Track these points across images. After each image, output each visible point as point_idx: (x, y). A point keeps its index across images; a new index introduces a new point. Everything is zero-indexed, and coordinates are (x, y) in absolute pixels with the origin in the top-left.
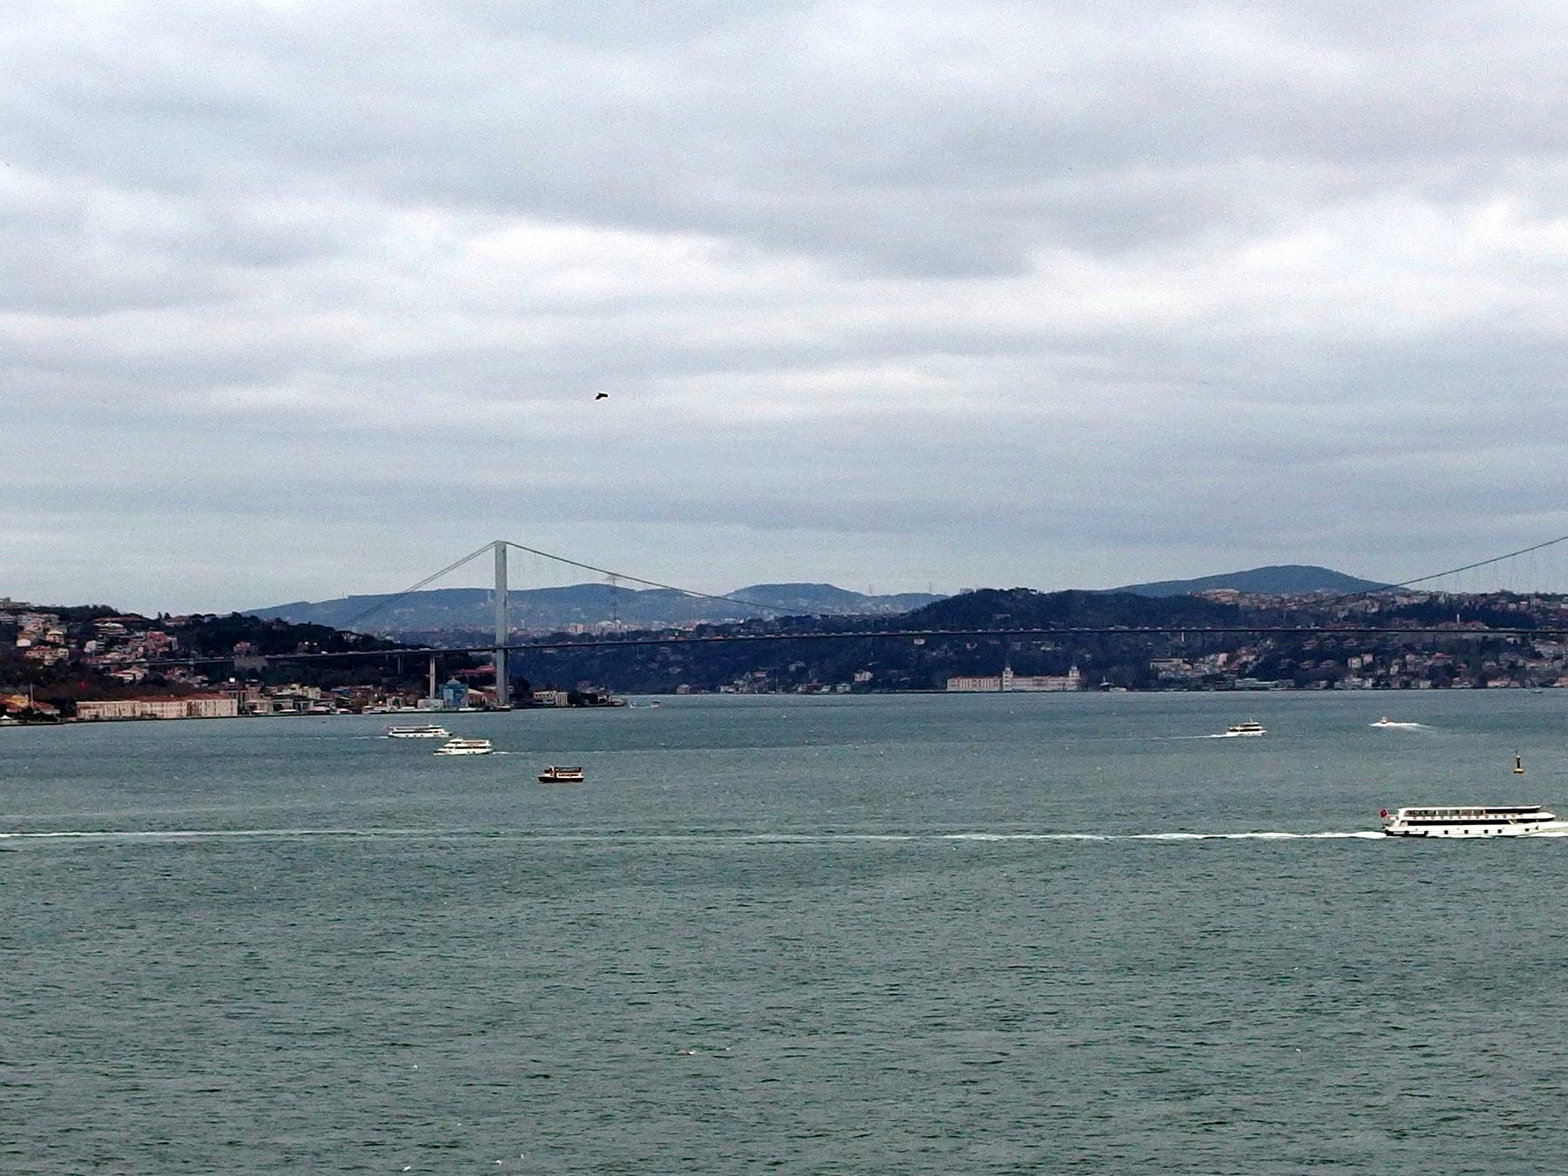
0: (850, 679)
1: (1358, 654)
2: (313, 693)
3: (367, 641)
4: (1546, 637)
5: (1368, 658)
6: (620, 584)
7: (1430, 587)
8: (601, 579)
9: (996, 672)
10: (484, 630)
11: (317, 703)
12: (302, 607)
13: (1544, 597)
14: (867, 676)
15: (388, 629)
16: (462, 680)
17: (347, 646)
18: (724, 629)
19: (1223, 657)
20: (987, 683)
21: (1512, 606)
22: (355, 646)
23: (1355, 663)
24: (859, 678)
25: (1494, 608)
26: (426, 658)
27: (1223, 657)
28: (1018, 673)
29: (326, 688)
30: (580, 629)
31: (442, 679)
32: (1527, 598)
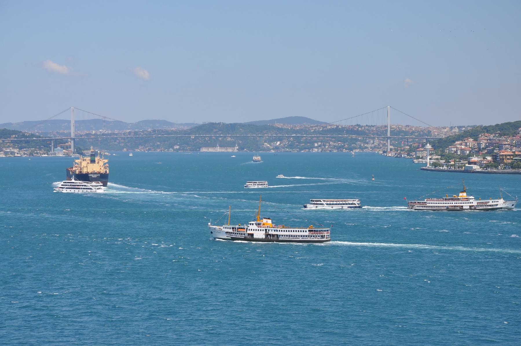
0: (173, 148)
1: (317, 142)
2: (16, 151)
3: (32, 135)
4: (370, 138)
5: (320, 144)
6: (106, 119)
7: (338, 124)
8: (100, 118)
9: (214, 146)
10: (66, 132)
11: (17, 154)
12: (10, 124)
13: (369, 126)
14: (178, 147)
15: (36, 131)
16: (61, 147)
17: (26, 137)
18: (136, 133)
19: (278, 143)
20: (211, 150)
21: (360, 129)
22: (28, 137)
23: (316, 145)
24: (175, 148)
25: (355, 129)
26: (51, 140)
27: (278, 143)
28: (221, 146)
29: (21, 148)
30: (94, 132)
31: (55, 147)
32: (363, 126)
